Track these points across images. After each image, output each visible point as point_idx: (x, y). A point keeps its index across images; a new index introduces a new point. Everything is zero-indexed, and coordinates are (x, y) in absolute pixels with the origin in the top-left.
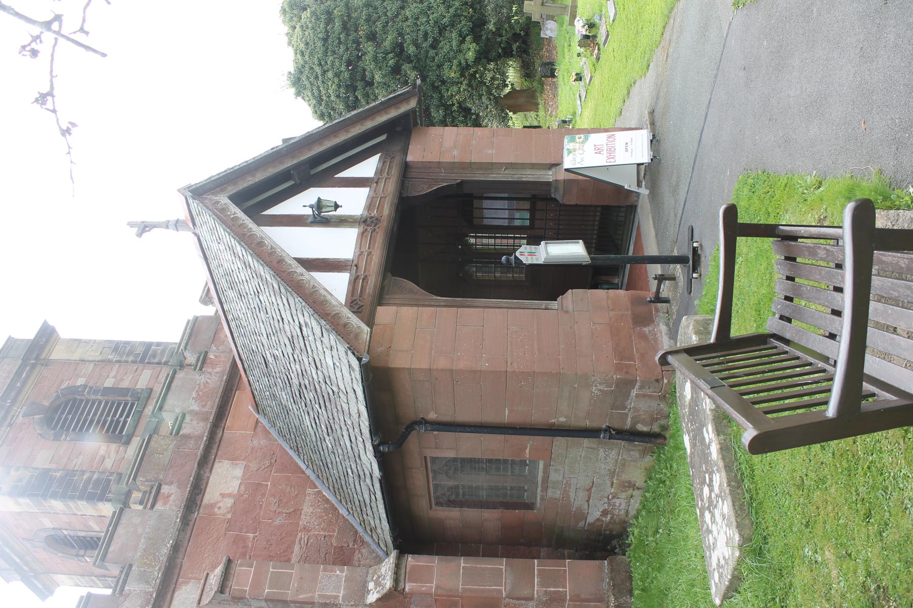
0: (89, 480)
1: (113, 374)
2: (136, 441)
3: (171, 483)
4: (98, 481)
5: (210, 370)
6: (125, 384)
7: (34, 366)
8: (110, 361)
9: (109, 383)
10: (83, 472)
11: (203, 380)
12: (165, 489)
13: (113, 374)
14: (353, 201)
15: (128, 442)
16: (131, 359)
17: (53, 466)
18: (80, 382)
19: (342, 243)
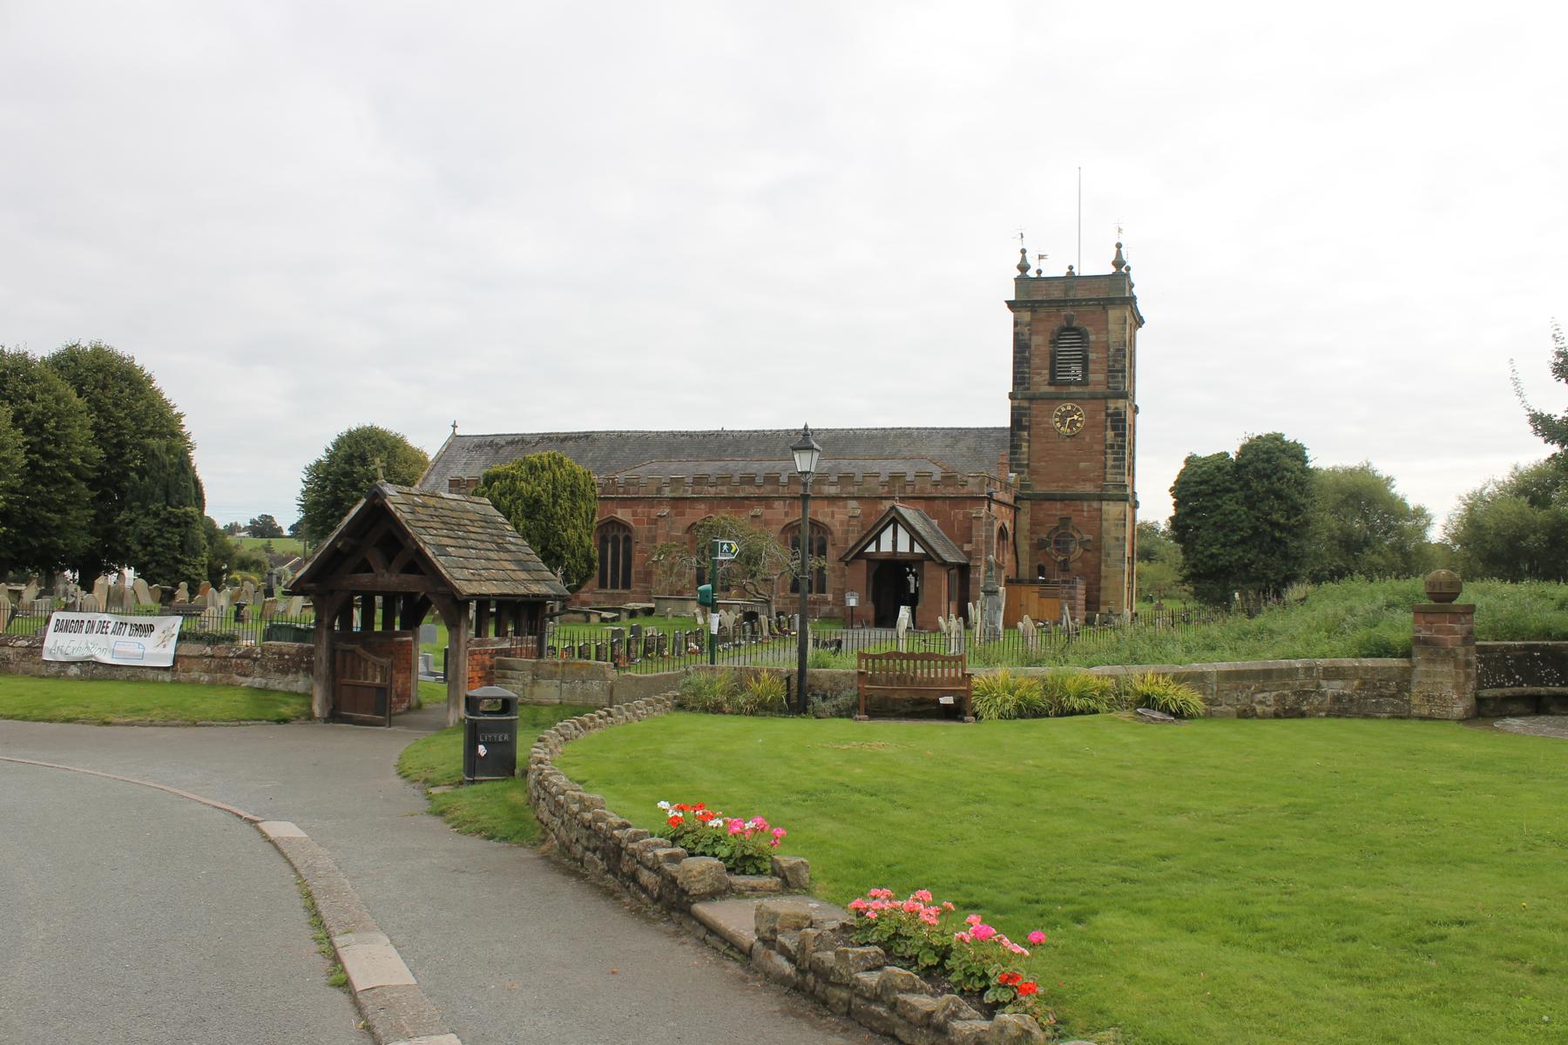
2: (1052, 389)
6: (1091, 366)
9: (1092, 356)
14: (904, 547)
18: (1092, 338)
19: (886, 546)
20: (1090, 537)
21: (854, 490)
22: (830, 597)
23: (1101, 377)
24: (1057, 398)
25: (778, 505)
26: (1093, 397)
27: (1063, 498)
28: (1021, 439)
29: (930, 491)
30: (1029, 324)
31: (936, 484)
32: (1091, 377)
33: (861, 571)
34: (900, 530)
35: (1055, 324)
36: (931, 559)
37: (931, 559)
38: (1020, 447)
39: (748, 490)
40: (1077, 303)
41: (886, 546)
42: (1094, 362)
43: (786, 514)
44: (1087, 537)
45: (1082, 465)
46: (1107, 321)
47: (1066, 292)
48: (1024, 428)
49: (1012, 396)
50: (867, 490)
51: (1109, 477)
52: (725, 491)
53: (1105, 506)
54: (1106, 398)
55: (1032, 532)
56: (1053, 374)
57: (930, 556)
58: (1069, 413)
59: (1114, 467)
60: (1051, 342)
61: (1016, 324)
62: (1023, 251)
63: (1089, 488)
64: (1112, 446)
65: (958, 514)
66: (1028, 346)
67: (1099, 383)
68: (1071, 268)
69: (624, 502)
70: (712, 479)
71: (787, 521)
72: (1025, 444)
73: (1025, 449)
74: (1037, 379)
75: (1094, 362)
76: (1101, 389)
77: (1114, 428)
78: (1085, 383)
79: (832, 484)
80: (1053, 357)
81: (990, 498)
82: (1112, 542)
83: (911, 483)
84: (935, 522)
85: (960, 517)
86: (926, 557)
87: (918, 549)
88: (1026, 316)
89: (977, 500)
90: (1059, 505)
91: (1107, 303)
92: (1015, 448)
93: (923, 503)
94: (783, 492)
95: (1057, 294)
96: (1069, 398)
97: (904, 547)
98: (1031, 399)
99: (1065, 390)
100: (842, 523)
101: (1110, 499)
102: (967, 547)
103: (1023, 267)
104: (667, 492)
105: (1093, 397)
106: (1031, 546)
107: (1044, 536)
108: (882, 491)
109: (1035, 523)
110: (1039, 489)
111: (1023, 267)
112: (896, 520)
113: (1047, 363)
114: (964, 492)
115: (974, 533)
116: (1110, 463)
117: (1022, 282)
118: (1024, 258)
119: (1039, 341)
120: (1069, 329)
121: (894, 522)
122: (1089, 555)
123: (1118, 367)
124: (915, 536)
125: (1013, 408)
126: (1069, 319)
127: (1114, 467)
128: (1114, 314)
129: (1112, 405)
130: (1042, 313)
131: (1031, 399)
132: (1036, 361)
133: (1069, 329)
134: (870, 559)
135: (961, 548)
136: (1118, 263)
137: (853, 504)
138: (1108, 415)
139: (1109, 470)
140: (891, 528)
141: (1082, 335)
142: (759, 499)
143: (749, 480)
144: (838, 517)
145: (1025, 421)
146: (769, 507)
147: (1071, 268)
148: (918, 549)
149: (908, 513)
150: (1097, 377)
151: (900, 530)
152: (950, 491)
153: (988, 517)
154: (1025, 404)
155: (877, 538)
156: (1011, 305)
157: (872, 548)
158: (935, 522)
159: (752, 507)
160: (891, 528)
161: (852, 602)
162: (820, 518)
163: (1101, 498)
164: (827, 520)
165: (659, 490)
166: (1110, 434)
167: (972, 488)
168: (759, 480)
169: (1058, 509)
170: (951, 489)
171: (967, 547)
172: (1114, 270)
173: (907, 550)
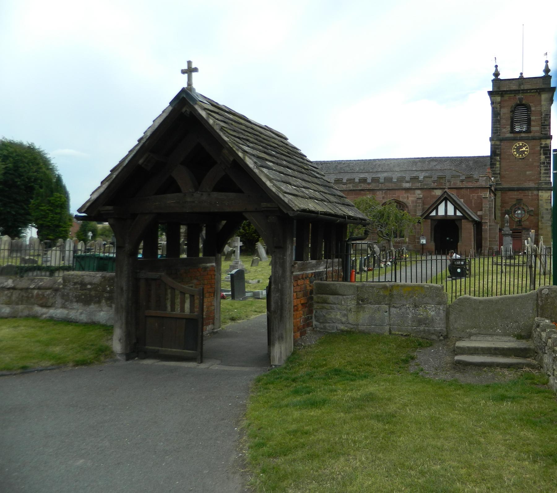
0: (497, 127)
1: (537, 118)
2: (512, 135)
4: (497, 130)
6: (532, 123)
7: (537, 92)
8: (542, 115)
9: (533, 118)
10: (500, 125)
13: (537, 118)
14: (451, 212)
15: (511, 133)
16: (543, 121)
17: (502, 114)
18: (533, 109)
19: (441, 212)
20: (533, 209)
21: (418, 185)
22: (407, 240)
23: (537, 128)
24: (515, 140)
26: (534, 139)
27: (519, 189)
28: (496, 160)
29: (459, 185)
30: (500, 103)
31: (462, 181)
32: (533, 129)
33: (427, 227)
34: (449, 204)
35: (513, 103)
36: (467, 219)
37: (467, 219)
38: (495, 164)
40: (525, 91)
41: (441, 212)
42: (534, 121)
44: (531, 209)
45: (528, 173)
46: (540, 101)
47: (520, 85)
48: (497, 155)
49: (491, 139)
50: (426, 185)
51: (542, 179)
53: (540, 193)
54: (541, 139)
55: (502, 206)
56: (512, 127)
57: (465, 217)
58: (521, 147)
59: (545, 173)
60: (511, 112)
61: (492, 103)
62: (496, 66)
63: (532, 185)
64: (544, 163)
66: (499, 114)
67: (536, 132)
68: (521, 74)
72: (498, 163)
73: (498, 166)
74: (504, 130)
75: (534, 121)
76: (538, 134)
77: (545, 154)
78: (528, 131)
79: (407, 182)
80: (512, 119)
82: (545, 211)
84: (462, 200)
87: (458, 213)
88: (498, 99)
90: (516, 193)
91: (540, 91)
92: (492, 165)
93: (455, 190)
95: (514, 87)
96: (521, 139)
97: (451, 212)
98: (501, 140)
99: (518, 136)
100: (413, 202)
101: (542, 189)
102: (479, 213)
103: (496, 74)
105: (534, 139)
106: (501, 214)
107: (509, 209)
108: (433, 185)
109: (503, 202)
110: (505, 185)
111: (496, 74)
112: (446, 199)
113: (509, 122)
115: (483, 205)
116: (543, 171)
117: (497, 81)
118: (497, 70)
119: (505, 112)
120: (521, 105)
121: (446, 199)
122: (532, 218)
123: (546, 123)
124: (457, 207)
125: (492, 145)
126: (521, 100)
127: (545, 173)
128: (544, 96)
129: (544, 142)
130: (506, 97)
131: (501, 140)
132: (503, 121)
133: (521, 105)
134: (433, 219)
136: (547, 70)
137: (418, 192)
138: (541, 147)
139: (542, 175)
140: (443, 203)
141: (528, 108)
142: (369, 190)
143: (364, 181)
144: (411, 199)
145: (498, 152)
147: (521, 74)
149: (453, 194)
150: (535, 128)
151: (449, 204)
152: (470, 185)
154: (498, 143)
155: (436, 208)
156: (490, 93)
157: (434, 213)
158: (462, 200)
159: (365, 195)
160: (444, 202)
161: (424, 241)
162: (401, 199)
163: (538, 189)
164: (405, 200)
166: (543, 157)
169: (515, 195)
170: (470, 184)
171: (479, 213)
172: (542, 74)
173: (453, 214)
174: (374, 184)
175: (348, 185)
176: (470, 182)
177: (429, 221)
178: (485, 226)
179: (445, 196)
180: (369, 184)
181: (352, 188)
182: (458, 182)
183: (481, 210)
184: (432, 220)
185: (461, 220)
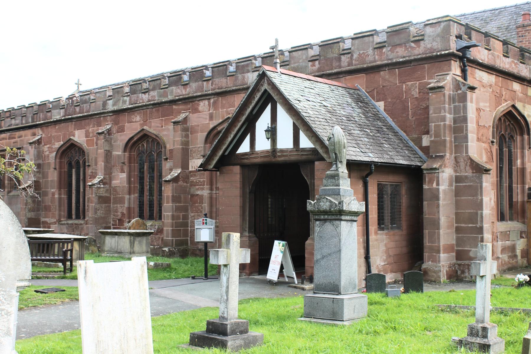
3: (319, 64)
5: (376, 53)
11: (369, 53)
12: (317, 62)
14: (285, 141)
25: (203, 105)
29: (373, 58)
31: (380, 47)
33: (231, 187)
34: (281, 111)
39: (177, 92)
43: (211, 117)
52: (155, 96)
57: (323, 153)
65: (413, 88)
69: (82, 120)
70: (145, 86)
71: (211, 126)
81: (463, 57)
83: (348, 52)
84: (381, 105)
85: (415, 93)
86: (313, 157)
87: (305, 143)
89: (440, 59)
94: (208, 88)
97: (285, 141)
102: (426, 141)
104: (110, 106)
114: (419, 51)
124: (301, 123)
135: (418, 141)
146: (196, 110)
148: (305, 143)
151: (281, 111)
152: (400, 54)
153: (457, 86)
155: (250, 127)
157: (244, 148)
158: (381, 105)
159: (179, 113)
165: (105, 104)
167: (431, 44)
168: (186, 78)
174: (194, 85)
175: (152, 93)
176: (400, 45)
177: (237, 169)
178: (431, 182)
179: (266, 86)
180: (185, 85)
181: (157, 99)
182: (370, 52)
183: (427, 133)
184: (244, 166)
185: (310, 163)
